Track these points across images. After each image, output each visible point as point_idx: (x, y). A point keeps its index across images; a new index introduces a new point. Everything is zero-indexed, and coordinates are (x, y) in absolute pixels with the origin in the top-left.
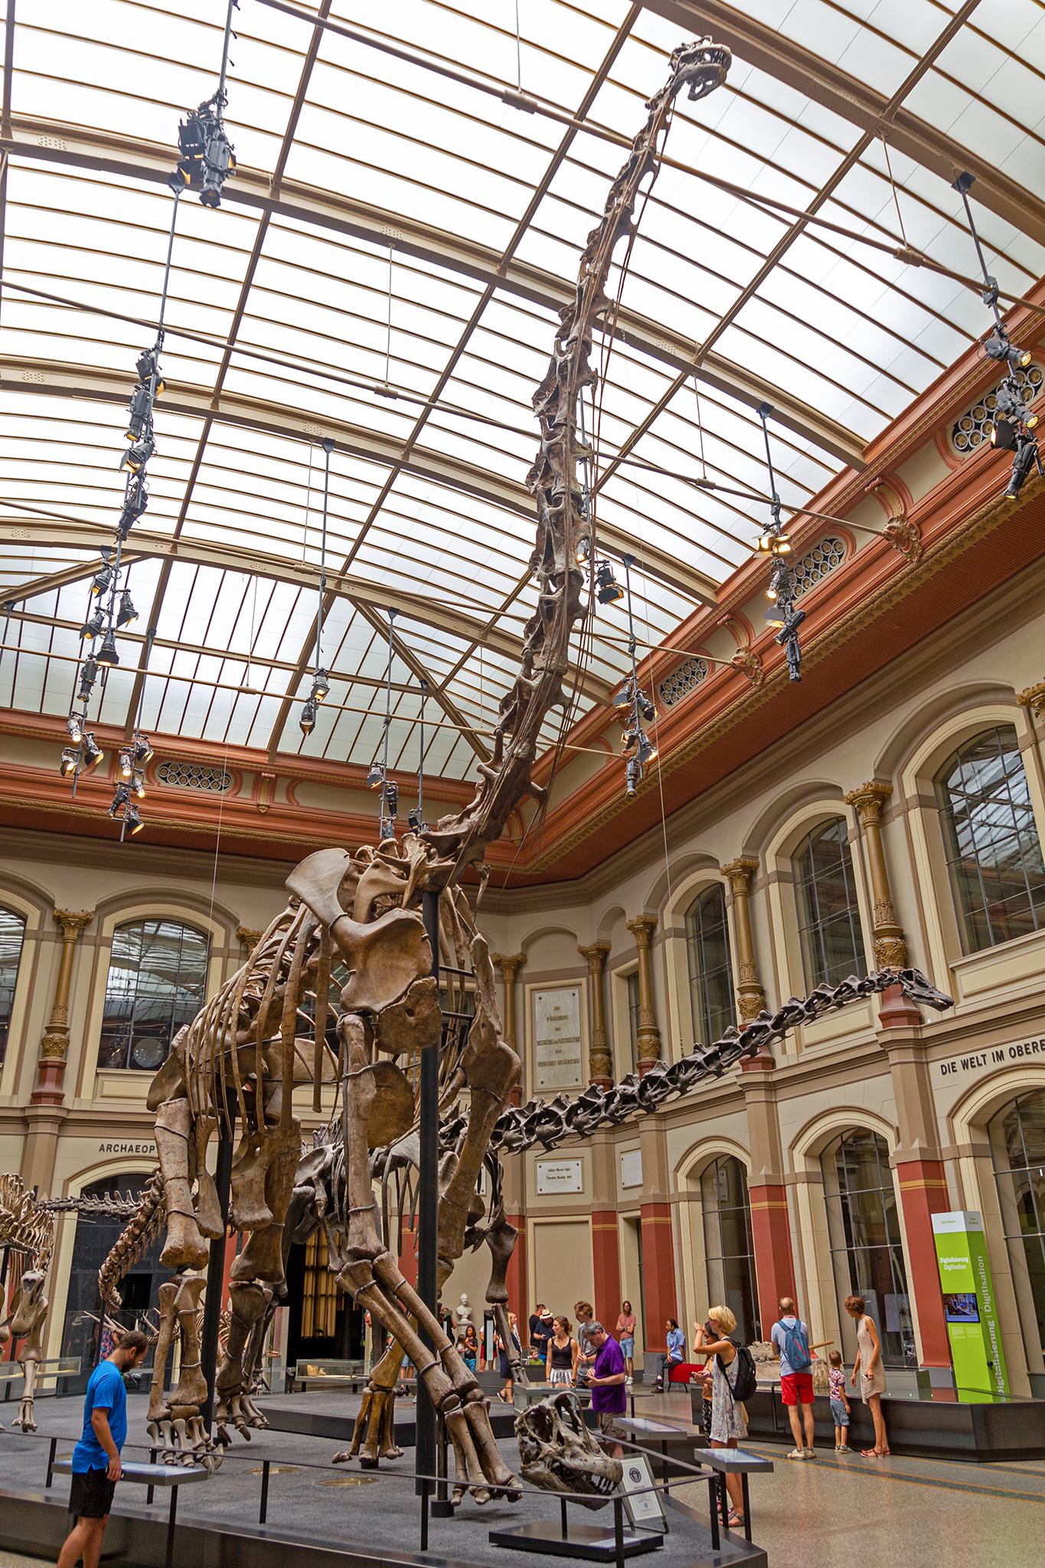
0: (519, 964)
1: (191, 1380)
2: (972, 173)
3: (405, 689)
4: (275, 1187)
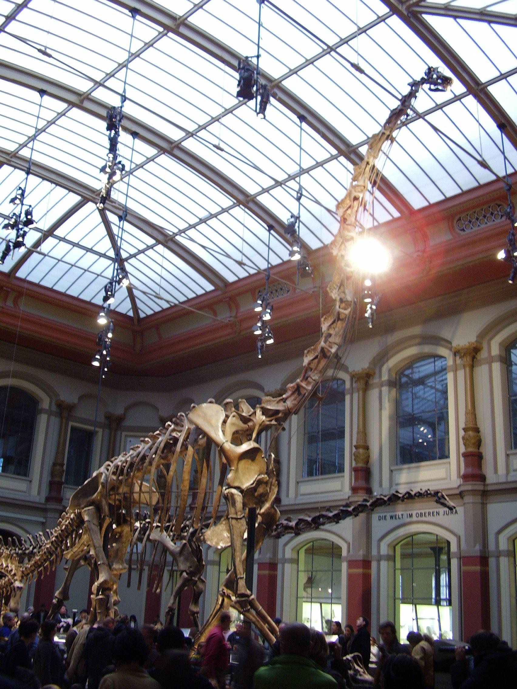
0: (120, 420)
2: (507, 124)
3: (104, 256)
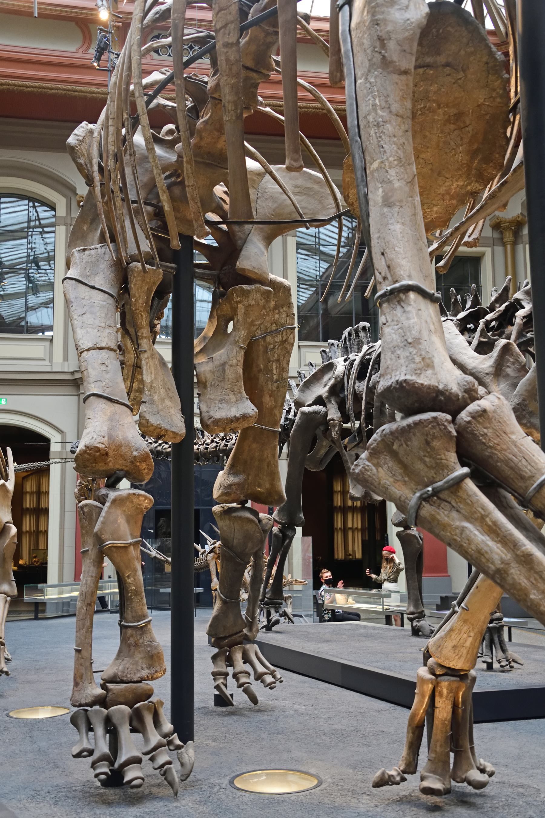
1: (136, 645)
4: (262, 378)
